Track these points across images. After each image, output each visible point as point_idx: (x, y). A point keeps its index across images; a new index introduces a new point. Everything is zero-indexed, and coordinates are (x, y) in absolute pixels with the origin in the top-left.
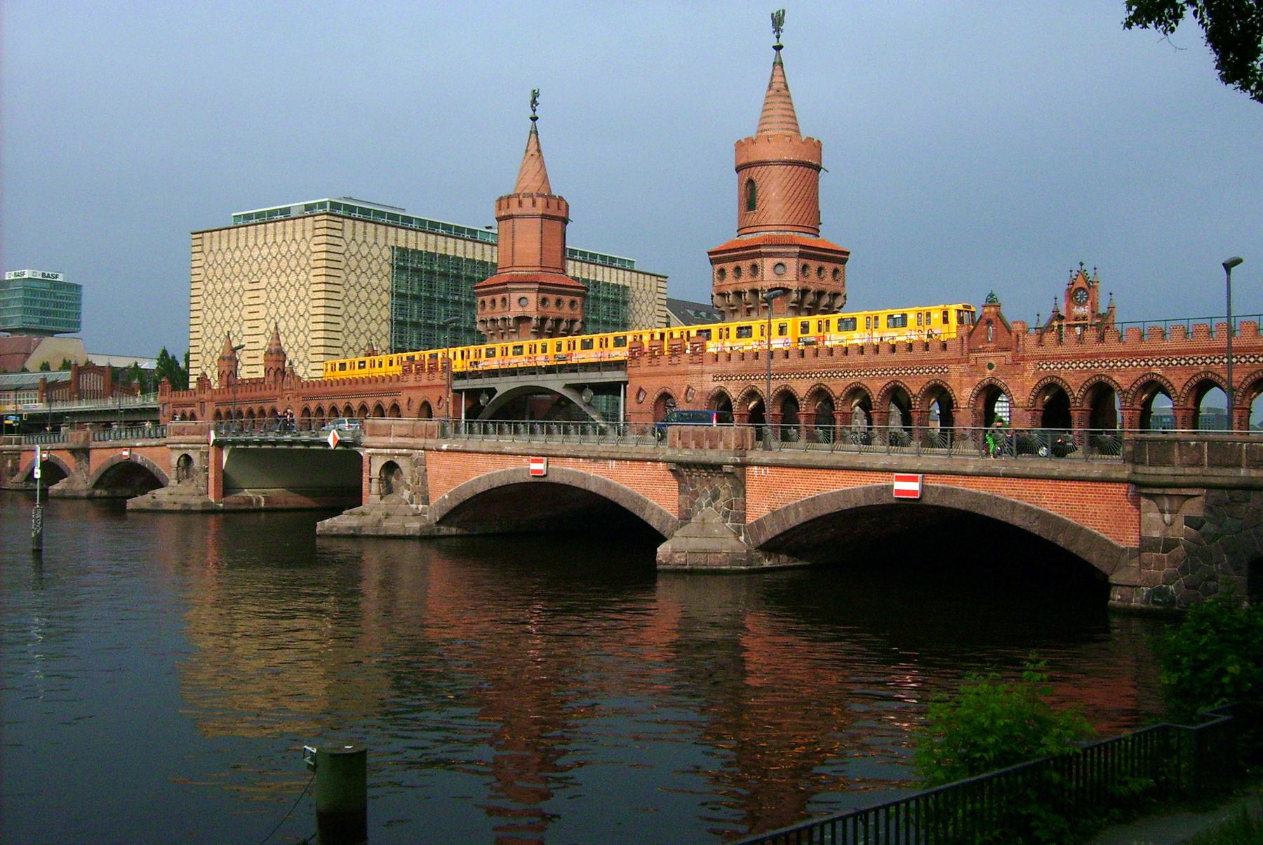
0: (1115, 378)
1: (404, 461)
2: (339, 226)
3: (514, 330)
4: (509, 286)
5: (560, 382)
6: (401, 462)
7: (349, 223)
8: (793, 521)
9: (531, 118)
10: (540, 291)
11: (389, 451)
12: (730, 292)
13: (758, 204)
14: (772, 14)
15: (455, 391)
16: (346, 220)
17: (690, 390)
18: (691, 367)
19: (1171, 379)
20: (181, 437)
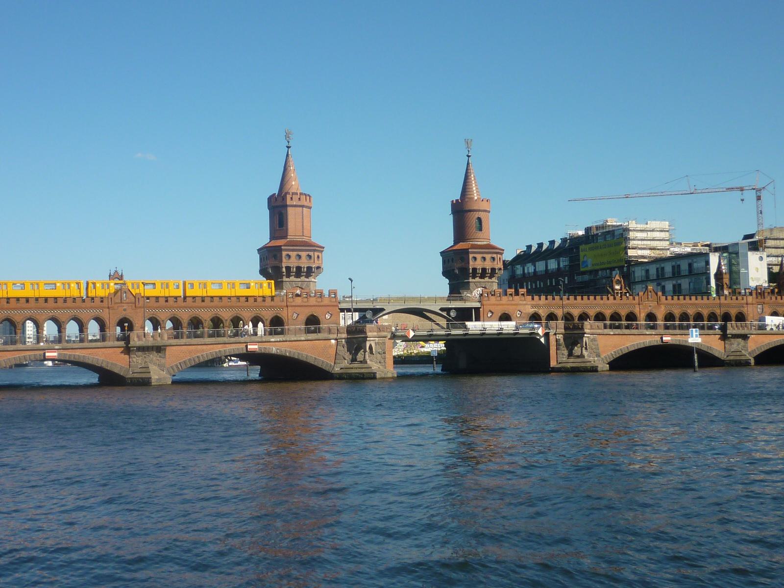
0: (688, 311)
8: (763, 350)
13: (483, 229)
18: (521, 302)
19: (703, 311)
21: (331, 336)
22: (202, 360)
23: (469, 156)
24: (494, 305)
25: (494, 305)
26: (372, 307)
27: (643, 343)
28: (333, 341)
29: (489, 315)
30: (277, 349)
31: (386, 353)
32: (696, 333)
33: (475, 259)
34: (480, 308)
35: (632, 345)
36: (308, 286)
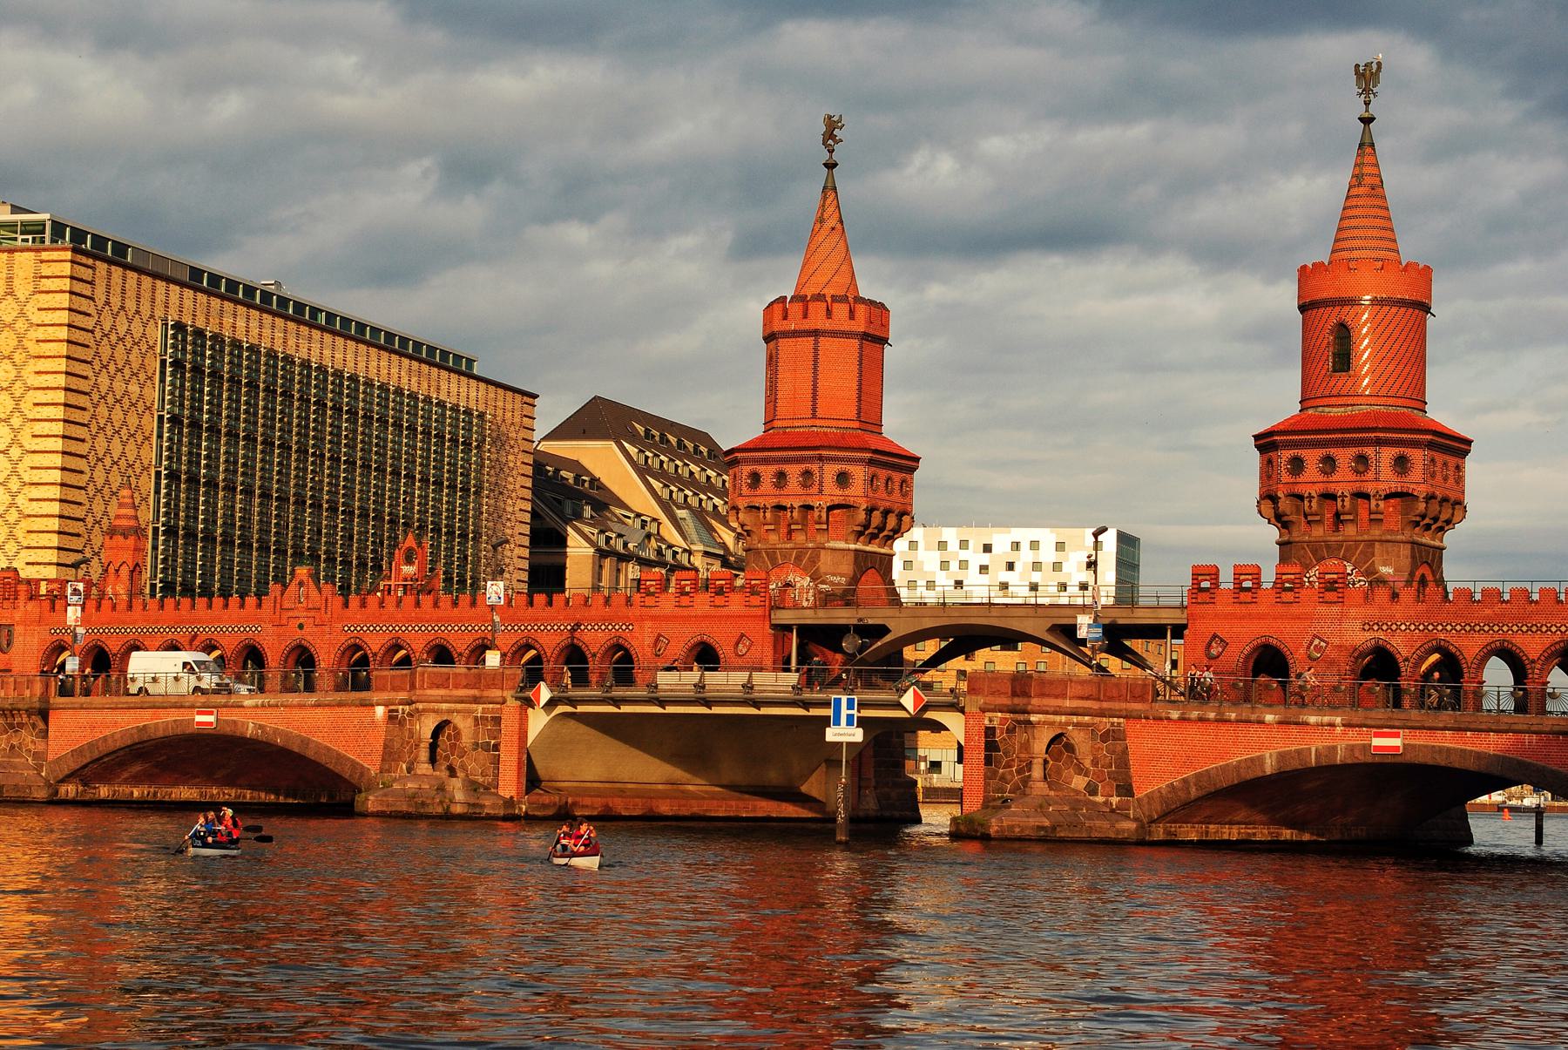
1: (1082, 734)
2: (86, 274)
3: (772, 527)
4: (824, 453)
5: (1041, 621)
6: (1078, 738)
7: (102, 267)
9: (826, 165)
10: (871, 462)
11: (1063, 718)
12: (1314, 494)
14: (1357, 66)
15: (775, 627)
16: (98, 263)
17: (1316, 642)
18: (1322, 609)
20: (442, 692)
21: (375, 696)
22: (111, 746)
23: (1367, 121)
24: (1228, 617)
25: (1228, 617)
26: (855, 622)
27: (1298, 752)
28: (380, 711)
29: (1214, 652)
30: (261, 727)
31: (502, 747)
32: (850, 712)
33: (1297, 465)
34: (1185, 627)
35: (1252, 760)
36: (814, 560)
